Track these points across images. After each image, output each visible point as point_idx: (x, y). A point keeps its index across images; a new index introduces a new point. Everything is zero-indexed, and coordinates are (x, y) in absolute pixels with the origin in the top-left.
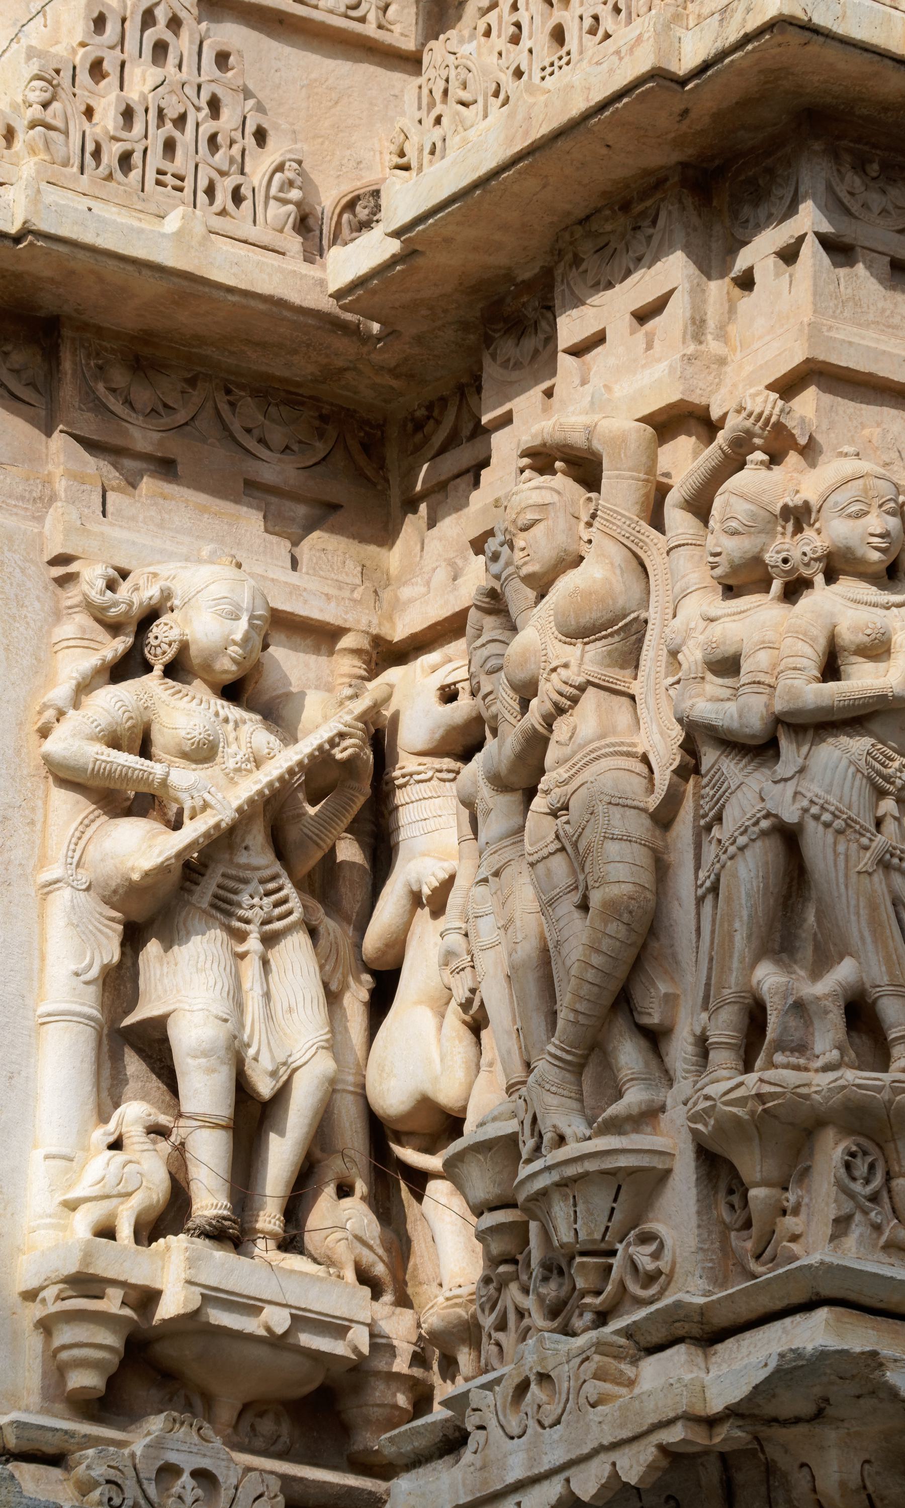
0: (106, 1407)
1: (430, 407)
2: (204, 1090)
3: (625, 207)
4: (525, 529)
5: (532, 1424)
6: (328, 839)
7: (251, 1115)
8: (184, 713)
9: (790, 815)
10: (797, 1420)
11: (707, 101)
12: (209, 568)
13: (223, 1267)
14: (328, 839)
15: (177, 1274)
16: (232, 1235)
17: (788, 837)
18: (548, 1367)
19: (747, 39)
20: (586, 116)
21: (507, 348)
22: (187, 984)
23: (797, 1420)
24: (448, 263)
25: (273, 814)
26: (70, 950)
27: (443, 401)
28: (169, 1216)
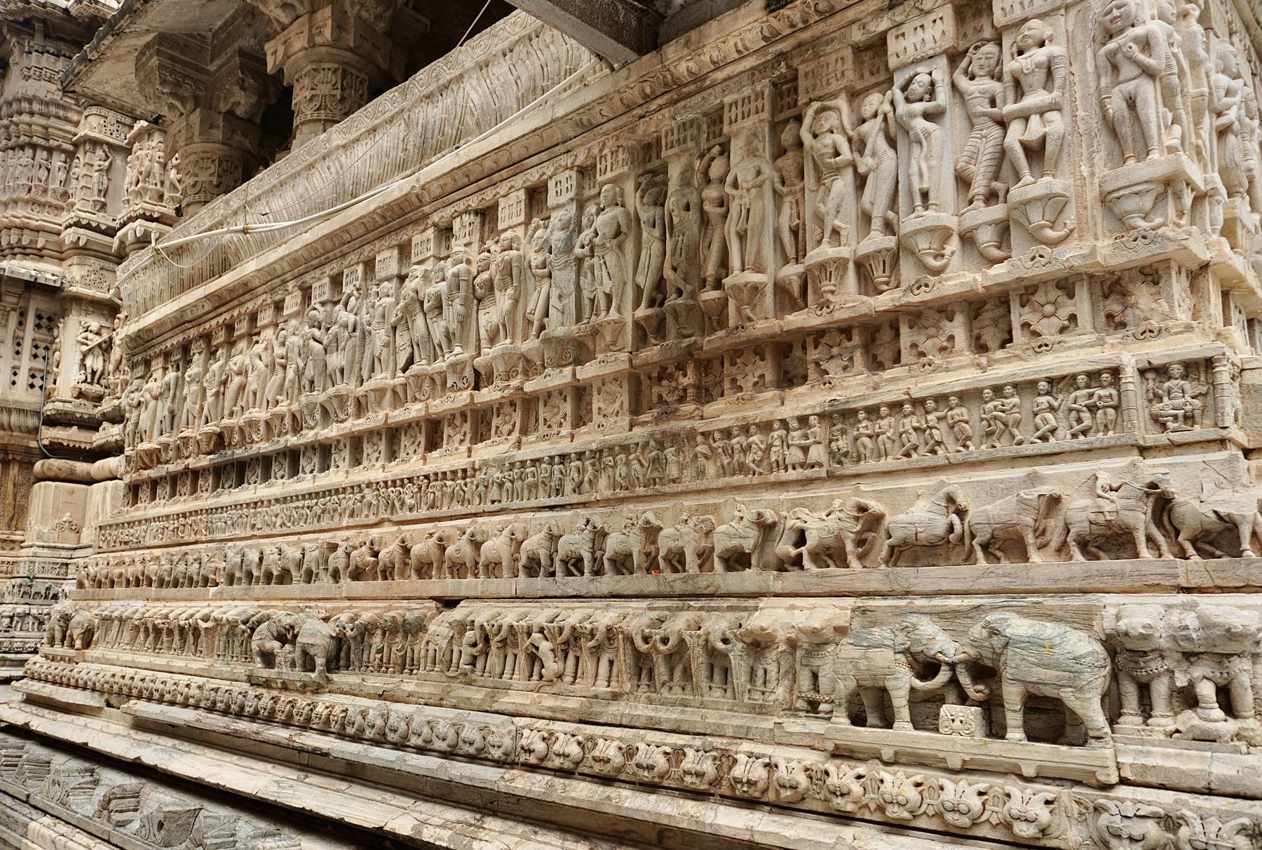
0: (78, 398)
2: (89, 370)
6: (106, 348)
7: (94, 373)
8: (90, 336)
12: (94, 324)
13: (89, 386)
14: (106, 348)
15: (84, 387)
16: (91, 383)
22: (89, 362)
25: (99, 345)
26: (79, 357)
28: (85, 381)
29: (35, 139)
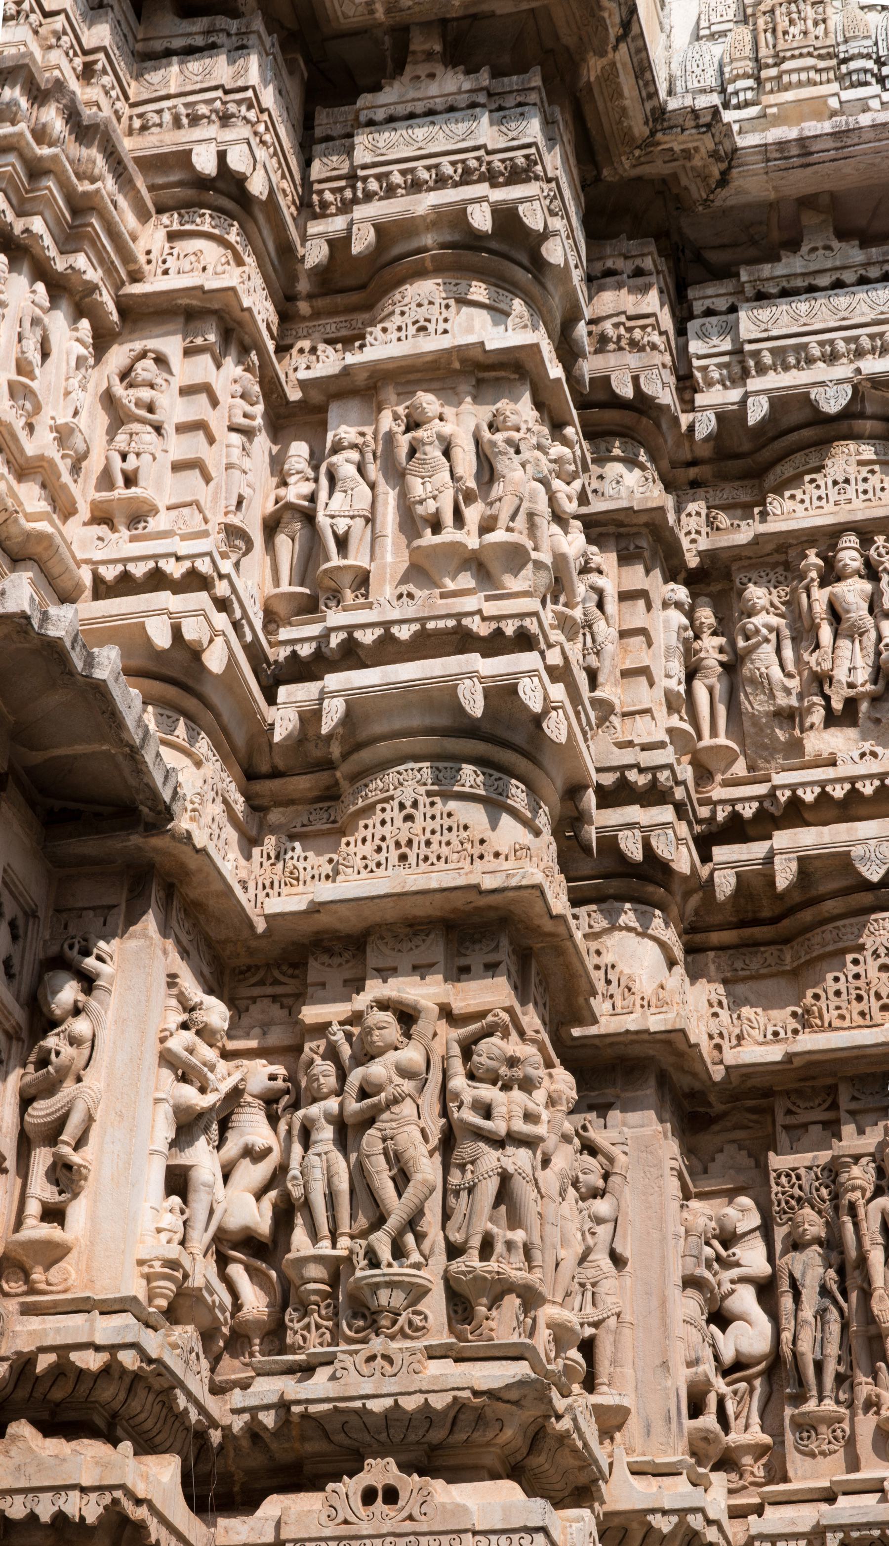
1: (249, 968)
3: (411, 926)
4: (380, 1028)
5: (378, 1374)
9: (511, 1169)
10: (508, 1402)
11: (483, 901)
17: (505, 1178)
18: (390, 1353)
19: (520, 888)
20: (435, 891)
21: (325, 958)
23: (508, 1402)
24: (324, 920)
27: (258, 968)
29: (37, 225)
